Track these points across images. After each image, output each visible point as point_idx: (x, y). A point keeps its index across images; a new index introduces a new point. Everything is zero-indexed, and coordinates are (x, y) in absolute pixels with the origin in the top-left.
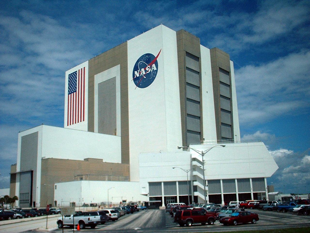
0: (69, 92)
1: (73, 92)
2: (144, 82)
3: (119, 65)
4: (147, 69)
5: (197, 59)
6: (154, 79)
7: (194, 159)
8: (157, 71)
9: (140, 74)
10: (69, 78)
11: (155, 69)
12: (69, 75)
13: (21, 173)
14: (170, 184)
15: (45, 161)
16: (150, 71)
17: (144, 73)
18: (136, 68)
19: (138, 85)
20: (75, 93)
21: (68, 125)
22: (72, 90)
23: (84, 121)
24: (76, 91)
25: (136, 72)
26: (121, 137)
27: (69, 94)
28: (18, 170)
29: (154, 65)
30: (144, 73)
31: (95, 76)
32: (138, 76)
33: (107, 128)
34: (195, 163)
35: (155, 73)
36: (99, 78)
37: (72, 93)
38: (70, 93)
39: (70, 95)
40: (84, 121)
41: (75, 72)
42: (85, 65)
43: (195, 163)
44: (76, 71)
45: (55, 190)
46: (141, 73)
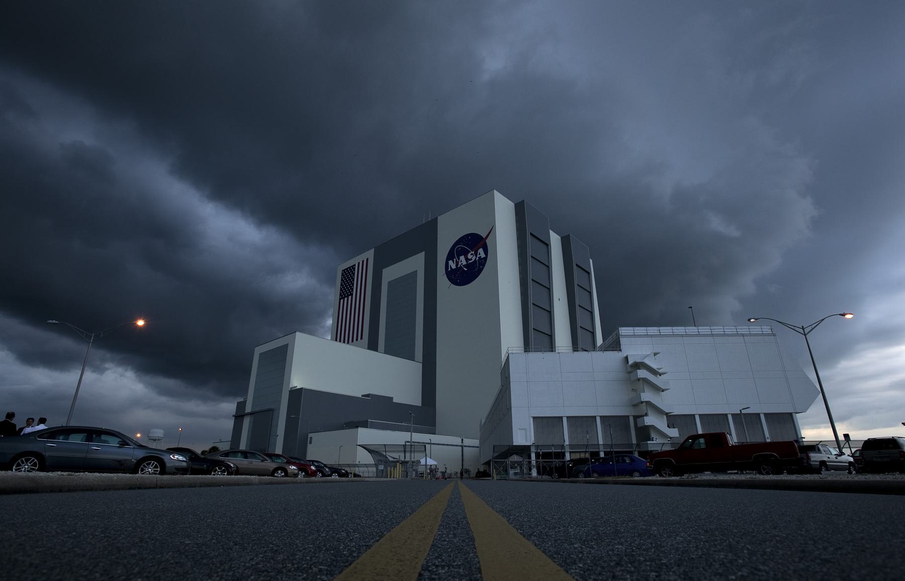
1: (348, 297)
2: (463, 277)
4: (469, 256)
5: (547, 245)
6: (480, 271)
7: (638, 366)
8: (485, 259)
9: (457, 265)
11: (483, 255)
13: (250, 414)
14: (581, 423)
15: (297, 394)
17: (464, 263)
18: (450, 257)
24: (352, 295)
25: (450, 262)
26: (423, 363)
28: (248, 409)
29: (481, 251)
30: (464, 263)
32: (454, 267)
33: (398, 347)
34: (642, 373)
35: (483, 262)
36: (391, 273)
42: (370, 254)
43: (642, 373)
45: (309, 446)
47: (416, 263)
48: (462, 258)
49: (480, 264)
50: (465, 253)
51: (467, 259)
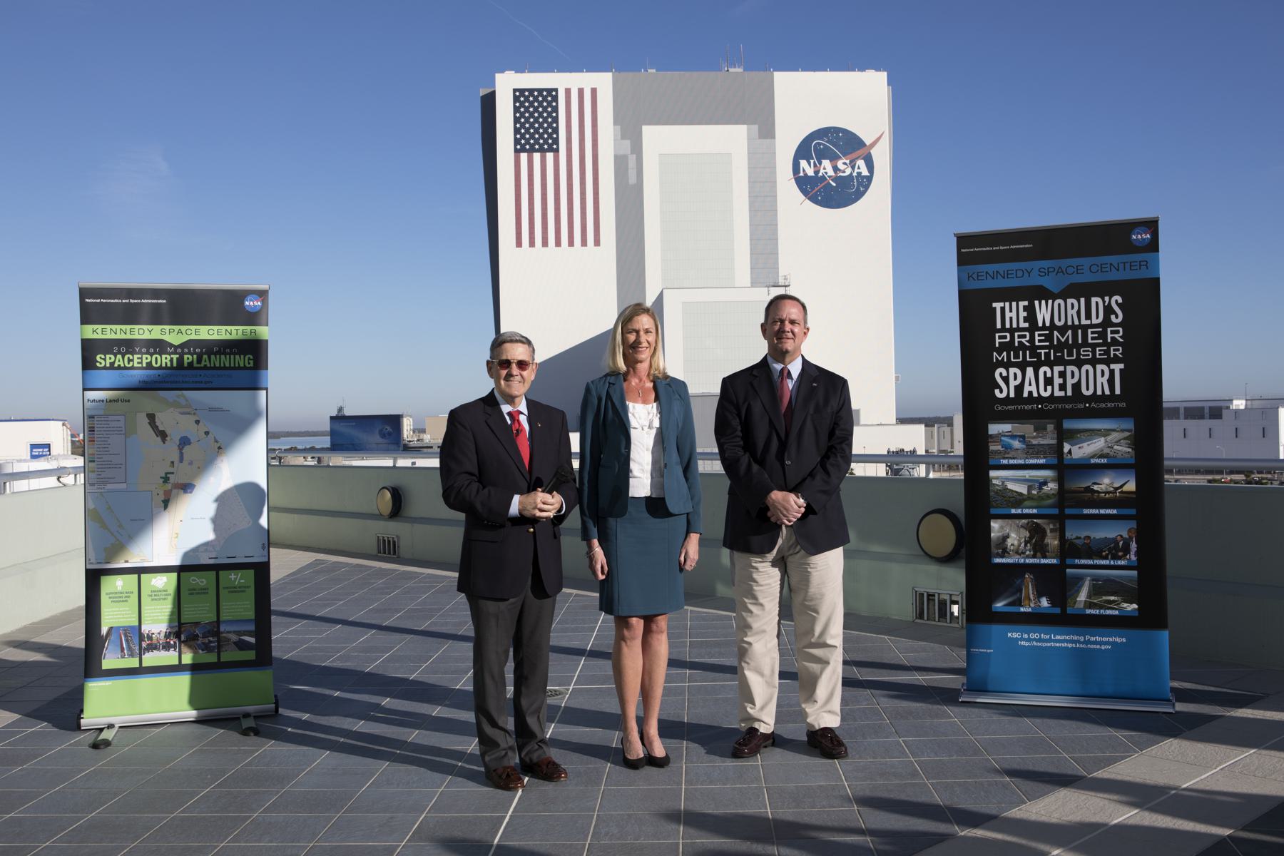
0: (517, 142)
3: (745, 127)
4: (840, 165)
6: (858, 195)
8: (870, 179)
9: (817, 172)
10: (516, 99)
11: (865, 172)
12: (515, 91)
16: (848, 171)
21: (519, 244)
22: (537, 141)
23: (597, 243)
24: (557, 151)
25: (803, 163)
27: (517, 151)
29: (861, 163)
30: (831, 173)
31: (645, 128)
32: (810, 172)
35: (864, 183)
37: (532, 150)
39: (524, 156)
40: (597, 243)
41: (549, 91)
44: (556, 90)
46: (822, 171)
47: (731, 139)
48: (826, 163)
49: (860, 184)
50: (834, 158)
51: (836, 169)
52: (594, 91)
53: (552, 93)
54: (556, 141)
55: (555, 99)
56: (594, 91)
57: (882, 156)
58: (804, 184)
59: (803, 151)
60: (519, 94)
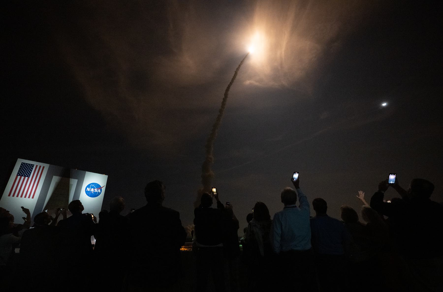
0: (18, 173)
1: (25, 176)
6: (98, 196)
8: (100, 193)
10: (22, 164)
11: (100, 192)
19: (88, 195)
20: (27, 178)
21: (9, 195)
25: (88, 188)
27: (17, 175)
31: (54, 176)
32: (89, 190)
35: (99, 194)
37: (22, 176)
38: (19, 175)
41: (32, 165)
48: (93, 189)
50: (94, 188)
52: (44, 167)
53: (33, 166)
54: (30, 175)
55: (33, 167)
56: (44, 167)
57: (104, 189)
58: (87, 192)
59: (88, 186)
60: (23, 164)
